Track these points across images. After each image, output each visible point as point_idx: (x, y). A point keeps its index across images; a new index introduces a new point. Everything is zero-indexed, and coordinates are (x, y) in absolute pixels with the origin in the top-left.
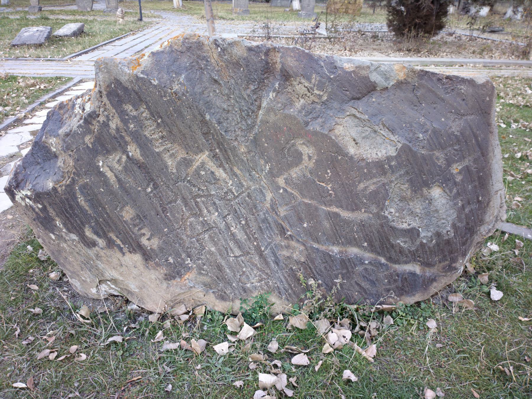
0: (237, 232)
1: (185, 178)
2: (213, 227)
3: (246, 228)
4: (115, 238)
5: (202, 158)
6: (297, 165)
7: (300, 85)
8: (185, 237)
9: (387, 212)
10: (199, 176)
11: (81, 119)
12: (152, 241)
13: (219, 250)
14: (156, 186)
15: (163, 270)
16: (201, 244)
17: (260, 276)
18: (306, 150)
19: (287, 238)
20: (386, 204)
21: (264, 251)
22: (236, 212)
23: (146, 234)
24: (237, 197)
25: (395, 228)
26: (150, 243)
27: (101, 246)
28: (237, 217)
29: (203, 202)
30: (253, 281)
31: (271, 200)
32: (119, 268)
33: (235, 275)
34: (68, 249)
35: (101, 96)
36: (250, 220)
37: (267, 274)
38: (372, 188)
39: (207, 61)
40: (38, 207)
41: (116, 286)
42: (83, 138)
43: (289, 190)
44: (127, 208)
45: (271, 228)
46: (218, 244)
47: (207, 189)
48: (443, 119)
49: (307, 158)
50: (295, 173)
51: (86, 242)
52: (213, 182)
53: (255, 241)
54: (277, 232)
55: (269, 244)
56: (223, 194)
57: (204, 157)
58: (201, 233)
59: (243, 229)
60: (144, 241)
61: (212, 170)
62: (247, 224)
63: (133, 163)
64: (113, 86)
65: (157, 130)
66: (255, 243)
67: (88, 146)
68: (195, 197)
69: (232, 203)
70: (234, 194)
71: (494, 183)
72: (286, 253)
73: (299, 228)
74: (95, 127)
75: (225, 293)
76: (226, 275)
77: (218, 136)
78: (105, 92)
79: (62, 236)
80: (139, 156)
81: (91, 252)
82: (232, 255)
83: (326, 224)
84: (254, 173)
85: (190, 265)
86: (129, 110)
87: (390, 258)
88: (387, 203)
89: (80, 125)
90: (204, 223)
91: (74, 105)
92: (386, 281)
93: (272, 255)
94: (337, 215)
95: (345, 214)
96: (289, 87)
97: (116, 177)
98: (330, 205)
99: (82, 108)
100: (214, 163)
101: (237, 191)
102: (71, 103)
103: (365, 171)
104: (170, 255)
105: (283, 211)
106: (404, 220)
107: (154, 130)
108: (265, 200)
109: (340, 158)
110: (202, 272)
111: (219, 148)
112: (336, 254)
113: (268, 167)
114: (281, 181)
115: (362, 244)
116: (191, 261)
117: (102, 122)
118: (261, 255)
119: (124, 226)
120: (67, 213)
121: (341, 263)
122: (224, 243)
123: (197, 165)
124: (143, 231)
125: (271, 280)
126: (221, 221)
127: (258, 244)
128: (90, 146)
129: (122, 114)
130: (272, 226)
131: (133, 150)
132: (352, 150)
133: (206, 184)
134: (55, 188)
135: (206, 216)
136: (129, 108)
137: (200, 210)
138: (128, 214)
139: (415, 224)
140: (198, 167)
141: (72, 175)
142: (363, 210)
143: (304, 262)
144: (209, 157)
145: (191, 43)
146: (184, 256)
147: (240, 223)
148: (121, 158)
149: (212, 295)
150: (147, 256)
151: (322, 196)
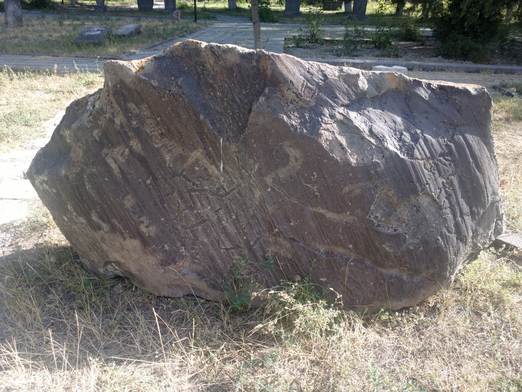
0: (228, 225)
1: (182, 173)
2: (206, 220)
3: (236, 222)
4: (117, 223)
5: (197, 155)
6: (284, 166)
7: (289, 91)
8: (179, 227)
9: (372, 217)
10: (194, 172)
11: (91, 115)
12: (150, 228)
13: (212, 243)
14: (155, 179)
15: (160, 256)
16: (195, 235)
17: (249, 268)
18: (293, 152)
19: (274, 235)
20: (372, 209)
21: (253, 246)
22: (227, 208)
23: (145, 221)
24: (229, 193)
25: (381, 232)
26: (148, 229)
27: (105, 230)
28: (229, 212)
29: (197, 196)
30: (242, 273)
31: (260, 198)
32: (121, 251)
33: (225, 266)
34: (78, 230)
35: (108, 95)
36: (240, 216)
37: (256, 267)
38: (358, 191)
39: (204, 66)
40: (53, 192)
41: (120, 268)
42: (92, 132)
43: (276, 189)
44: (128, 197)
45: (260, 224)
46: (210, 236)
47: (201, 184)
48: (434, 129)
49: (294, 160)
50: (282, 173)
51: (92, 225)
52: (207, 178)
53: (245, 235)
54: (265, 228)
55: (259, 239)
56: (215, 189)
57: (198, 154)
58: (195, 225)
59: (234, 224)
60: (143, 228)
61: (206, 167)
62: (237, 219)
63: (135, 156)
64: (119, 86)
65: (156, 128)
66: (245, 238)
67: (95, 140)
68: (189, 192)
69: (224, 198)
70: (225, 191)
71: (489, 195)
73: (286, 226)
74: (102, 122)
75: (216, 282)
76: (217, 265)
77: (211, 136)
78: (111, 92)
79: (73, 219)
80: (140, 150)
81: (98, 235)
82: (223, 247)
84: (244, 171)
85: (184, 254)
86: (132, 109)
87: (376, 262)
88: (372, 207)
89: (90, 120)
91: (87, 102)
92: (372, 283)
93: (260, 250)
94: (322, 216)
95: (330, 215)
96: (279, 93)
97: (120, 168)
98: (316, 206)
99: (93, 105)
100: (207, 161)
101: (229, 187)
102: (85, 100)
103: (351, 175)
104: (167, 243)
105: (270, 209)
106: (390, 226)
107: (153, 127)
108: (254, 197)
109: (325, 161)
110: (196, 261)
111: (212, 147)
112: (322, 254)
113: (256, 167)
114: (269, 180)
115: (347, 245)
116: (185, 250)
117: (108, 118)
119: (126, 214)
120: (77, 199)
121: (326, 262)
122: (216, 235)
123: (191, 161)
124: (142, 219)
125: (260, 273)
126: (214, 214)
127: (247, 239)
128: (98, 139)
129: (126, 111)
130: (261, 222)
131: (135, 144)
133: (200, 179)
134: (67, 175)
135: (199, 209)
136: (131, 106)
137: (194, 203)
138: (129, 202)
140: (193, 163)
141: (82, 165)
142: (348, 213)
143: (291, 259)
144: (202, 153)
145: (190, 50)
146: (178, 244)
147: (231, 218)
148: (124, 151)
149: (205, 284)
150: (145, 242)
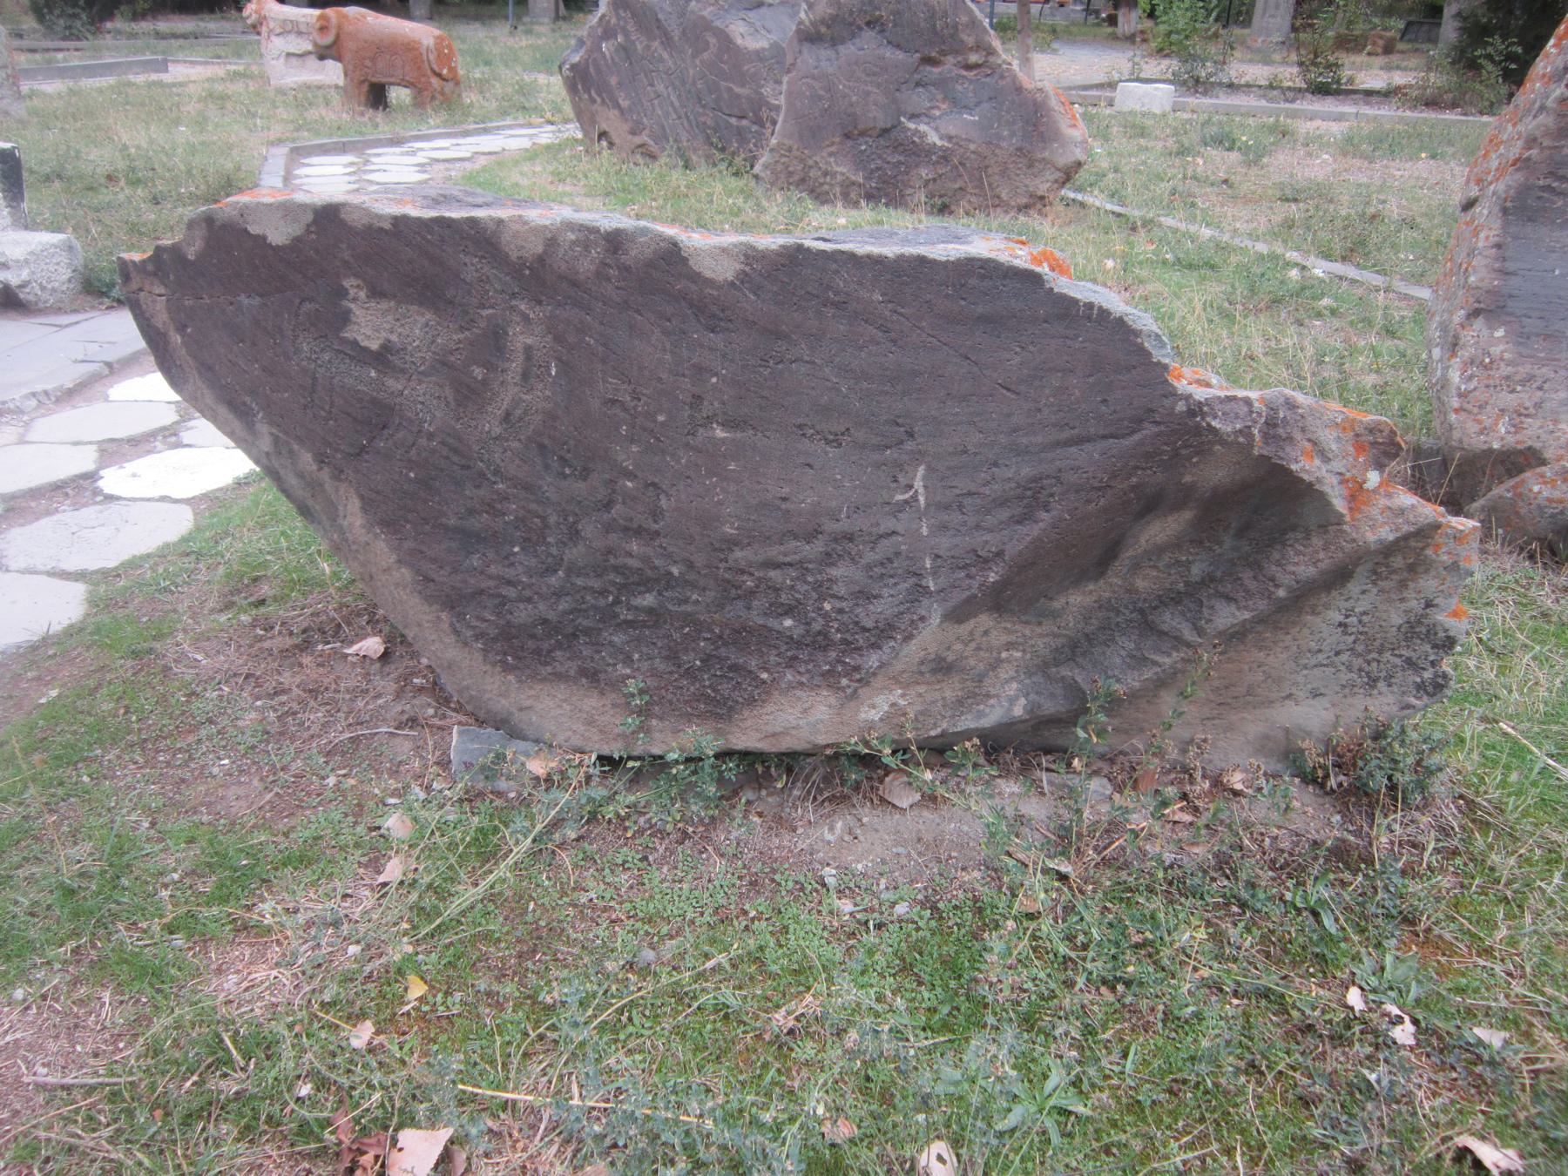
18: (713, 41)
26: (624, 103)
50: (706, 55)
57: (656, 44)
72: (703, 119)
83: (726, 95)
114: (697, 61)
129: (617, 14)
132: (739, 41)
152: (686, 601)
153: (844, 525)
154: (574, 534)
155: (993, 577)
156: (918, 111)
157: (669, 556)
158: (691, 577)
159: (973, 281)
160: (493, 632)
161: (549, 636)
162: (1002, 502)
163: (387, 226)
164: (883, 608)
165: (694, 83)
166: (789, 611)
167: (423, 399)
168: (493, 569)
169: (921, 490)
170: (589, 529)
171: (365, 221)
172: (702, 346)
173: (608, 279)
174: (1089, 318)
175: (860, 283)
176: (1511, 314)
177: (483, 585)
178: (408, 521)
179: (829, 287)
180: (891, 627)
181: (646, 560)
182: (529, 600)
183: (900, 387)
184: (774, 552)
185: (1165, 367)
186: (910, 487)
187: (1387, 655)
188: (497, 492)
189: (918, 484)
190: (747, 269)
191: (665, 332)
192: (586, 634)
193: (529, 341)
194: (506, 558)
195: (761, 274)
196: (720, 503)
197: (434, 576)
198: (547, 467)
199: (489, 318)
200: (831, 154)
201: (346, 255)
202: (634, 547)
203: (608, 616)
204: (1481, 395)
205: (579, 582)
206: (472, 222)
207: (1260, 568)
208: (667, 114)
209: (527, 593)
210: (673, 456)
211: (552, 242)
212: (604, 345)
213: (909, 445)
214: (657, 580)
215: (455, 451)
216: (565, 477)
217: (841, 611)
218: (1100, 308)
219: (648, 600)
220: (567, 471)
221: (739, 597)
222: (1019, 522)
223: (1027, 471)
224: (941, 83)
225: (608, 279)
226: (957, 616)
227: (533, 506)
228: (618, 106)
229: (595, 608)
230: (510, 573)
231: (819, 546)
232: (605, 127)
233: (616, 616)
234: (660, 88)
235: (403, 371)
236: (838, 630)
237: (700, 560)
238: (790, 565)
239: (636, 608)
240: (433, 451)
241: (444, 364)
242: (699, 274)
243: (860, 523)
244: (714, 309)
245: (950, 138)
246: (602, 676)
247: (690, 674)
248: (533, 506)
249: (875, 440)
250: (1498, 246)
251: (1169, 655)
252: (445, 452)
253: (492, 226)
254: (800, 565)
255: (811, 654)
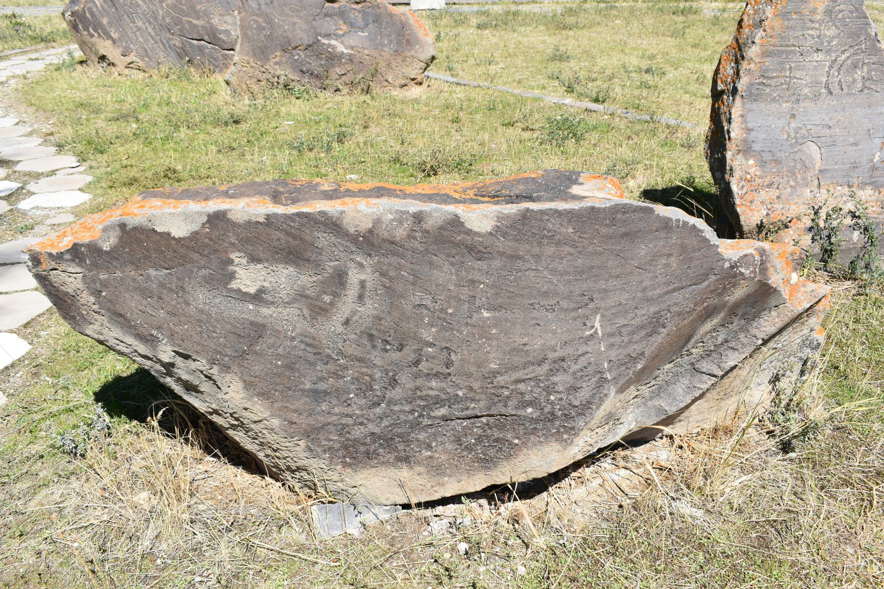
3: (154, 29)
14: (116, 9)
15: (121, 49)
26: (115, 36)
28: (150, 23)
60: (112, 34)
72: (173, 42)
90: (136, 27)
94: (190, 22)
105: (167, 20)
118: (163, 44)
139: (229, 27)
150: (114, 42)
151: (181, 12)
152: (467, 409)
153: (559, 354)
154: (394, 382)
155: (639, 366)
156: (329, 32)
157: (457, 386)
158: (471, 395)
159: (619, 216)
160: (337, 446)
161: (375, 442)
162: (642, 327)
163: (262, 220)
164: (583, 394)
165: (163, 18)
166: (530, 404)
167: (287, 318)
168: (336, 410)
169: (599, 328)
170: (404, 378)
171: (246, 218)
172: (474, 269)
173: (415, 238)
174: (678, 226)
175: (561, 225)
176: (755, 151)
177: (329, 420)
178: (276, 391)
179: (544, 229)
180: (589, 403)
181: (442, 390)
182: (361, 424)
183: (585, 276)
184: (520, 374)
185: (717, 246)
186: (593, 327)
187: (792, 358)
188: (339, 365)
189: (597, 325)
190: (499, 224)
191: (452, 264)
192: (399, 437)
193: (363, 278)
194: (345, 402)
195: (507, 227)
196: (488, 352)
197: (294, 420)
198: (374, 347)
199: (335, 268)
200: (276, 64)
201: (233, 240)
202: (434, 384)
203: (416, 425)
204: (749, 197)
205: (396, 408)
206: (323, 213)
207: (748, 331)
208: (146, 41)
209: (360, 420)
210: (458, 331)
211: (377, 222)
212: (414, 275)
213: (591, 305)
214: (449, 400)
215: (310, 345)
216: (387, 351)
217: (561, 399)
218: (683, 221)
219: (443, 411)
220: (388, 347)
221: (500, 401)
222: (650, 336)
223: (653, 309)
224: (342, 14)
225: (415, 238)
226: (621, 390)
227: (364, 370)
228: (109, 37)
229: (406, 422)
230: (349, 410)
231: (546, 367)
232: (102, 52)
233: (419, 423)
234: (140, 24)
235: (272, 303)
236: (560, 410)
237: (476, 385)
238: (530, 379)
239: (434, 417)
240: (296, 347)
241: (302, 296)
242: (471, 230)
243: (569, 350)
244: (481, 248)
245: (352, 48)
246: (412, 459)
247: (469, 448)
248: (364, 370)
249: (572, 306)
250: (742, 116)
251: (707, 383)
252: (303, 346)
253: (336, 215)
254: (536, 379)
255: (544, 425)
